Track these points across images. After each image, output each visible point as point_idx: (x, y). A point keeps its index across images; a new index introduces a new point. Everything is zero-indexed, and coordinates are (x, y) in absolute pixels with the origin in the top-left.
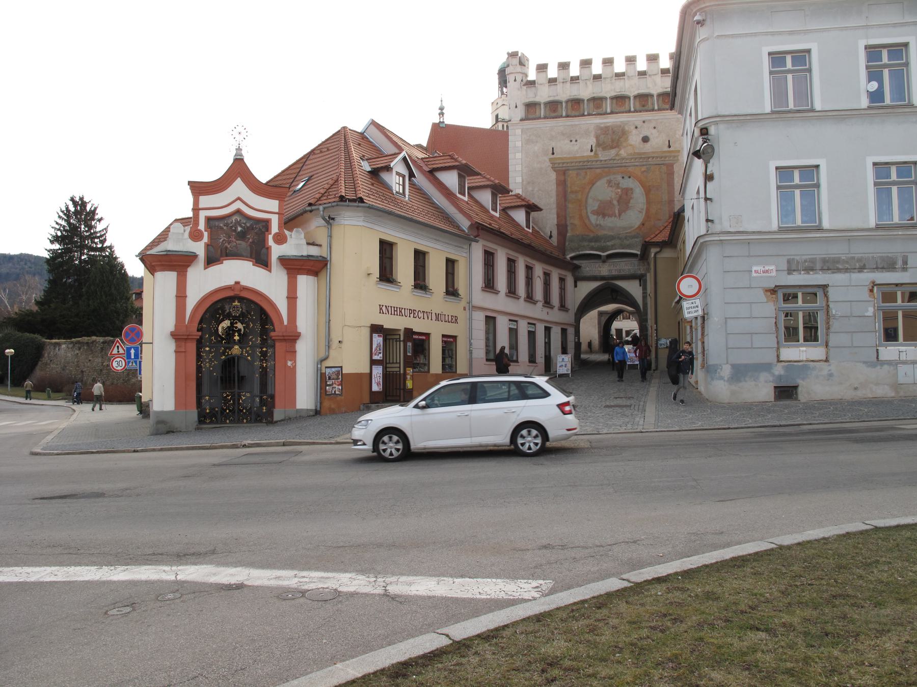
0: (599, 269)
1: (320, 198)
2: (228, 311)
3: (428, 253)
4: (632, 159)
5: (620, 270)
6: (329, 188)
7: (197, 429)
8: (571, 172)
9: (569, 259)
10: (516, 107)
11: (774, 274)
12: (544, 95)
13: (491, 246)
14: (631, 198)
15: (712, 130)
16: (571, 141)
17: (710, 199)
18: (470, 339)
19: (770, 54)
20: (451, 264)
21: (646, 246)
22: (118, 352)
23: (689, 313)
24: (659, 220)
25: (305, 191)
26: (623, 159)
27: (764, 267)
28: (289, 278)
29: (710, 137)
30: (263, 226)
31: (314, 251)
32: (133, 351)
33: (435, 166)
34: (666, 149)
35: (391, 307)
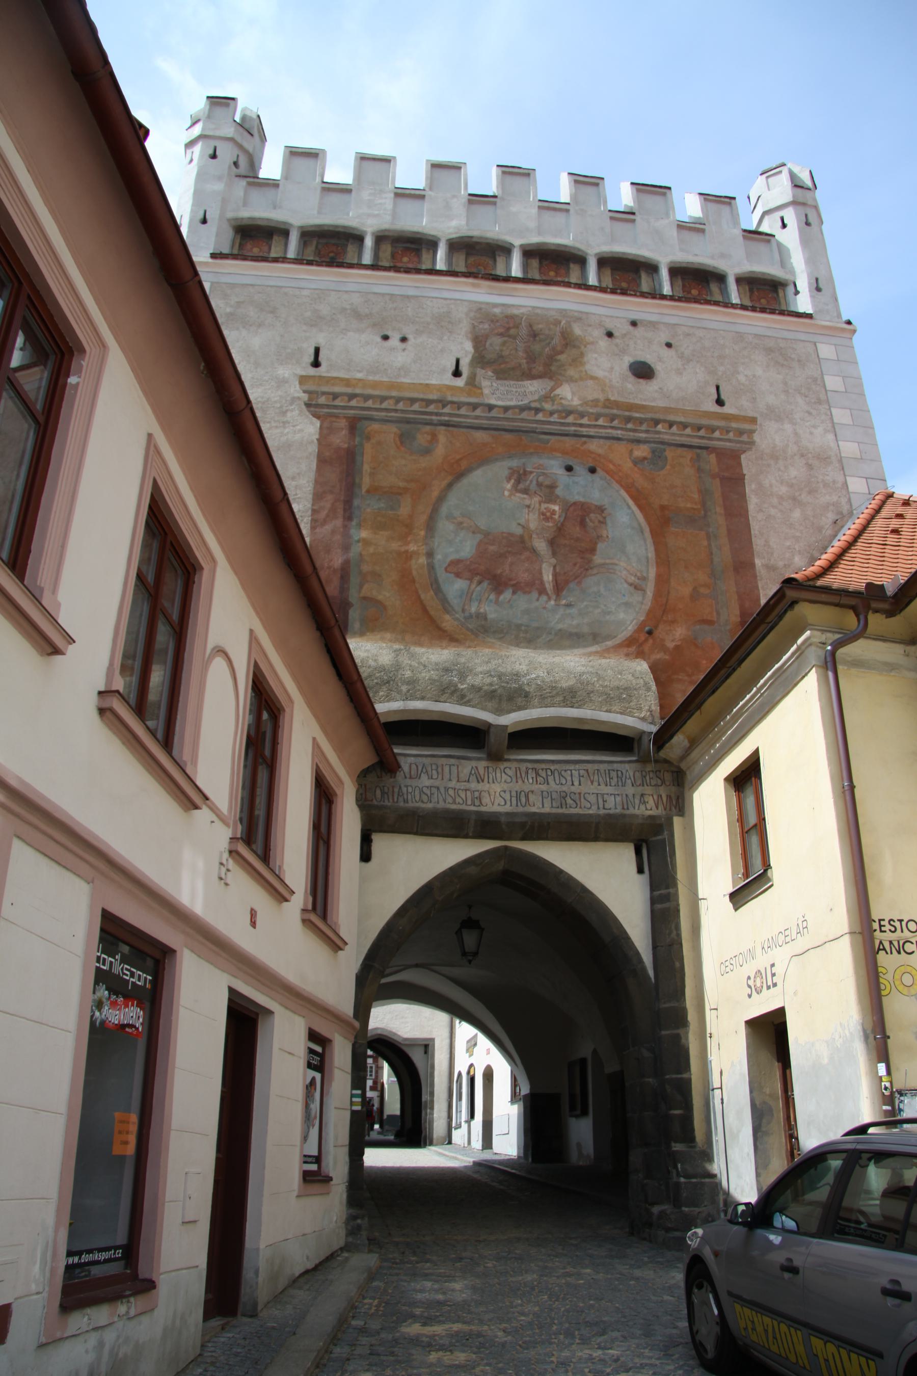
0: (473, 785)
4: (597, 417)
5: (564, 796)
8: (375, 426)
10: (204, 221)
14: (599, 537)
16: (386, 338)
24: (710, 622)
26: (569, 413)
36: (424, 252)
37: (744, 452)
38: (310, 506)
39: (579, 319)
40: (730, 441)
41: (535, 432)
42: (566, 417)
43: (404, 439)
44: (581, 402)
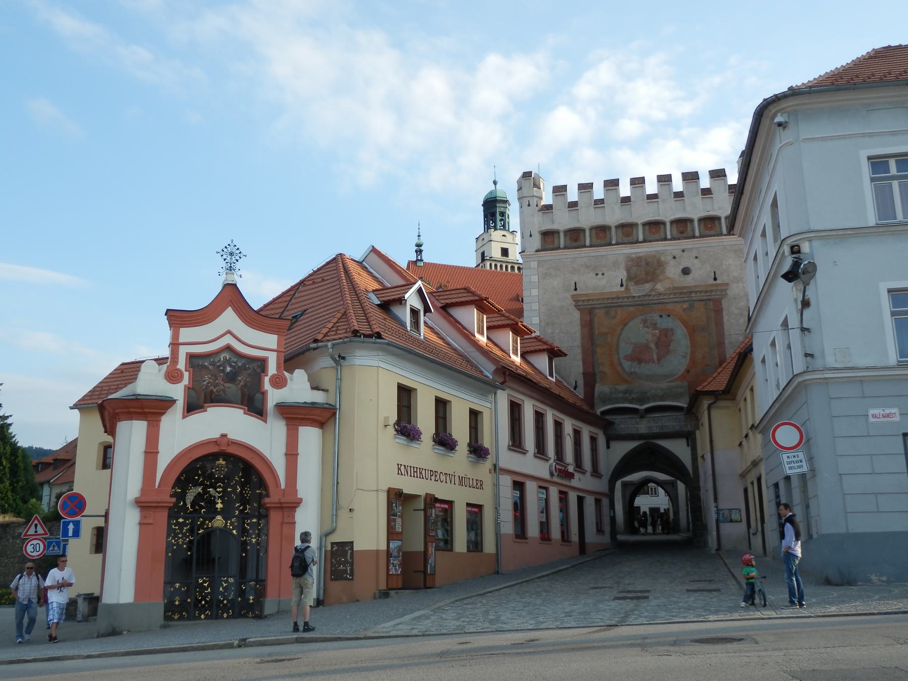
0: (636, 426)
1: (327, 333)
2: (209, 471)
3: (450, 401)
4: (670, 294)
6: (337, 323)
7: (164, 627)
8: (597, 311)
9: (599, 414)
10: (531, 236)
11: (897, 418)
12: (563, 221)
13: (519, 397)
14: (672, 340)
15: (805, 248)
16: (597, 275)
17: (808, 330)
18: (497, 509)
19: (869, 158)
20: (474, 415)
21: (696, 397)
22: (36, 532)
23: (791, 468)
25: (300, 327)
26: (660, 294)
27: (883, 410)
28: (288, 430)
29: (802, 256)
30: (258, 366)
31: (318, 397)
32: (71, 527)
33: (448, 301)
34: (712, 282)
35: (411, 467)
36: (607, 230)
37: (723, 299)
38: (580, 342)
39: (663, 253)
40: (718, 295)
41: (649, 304)
42: (659, 297)
43: (607, 313)
44: (664, 290)
